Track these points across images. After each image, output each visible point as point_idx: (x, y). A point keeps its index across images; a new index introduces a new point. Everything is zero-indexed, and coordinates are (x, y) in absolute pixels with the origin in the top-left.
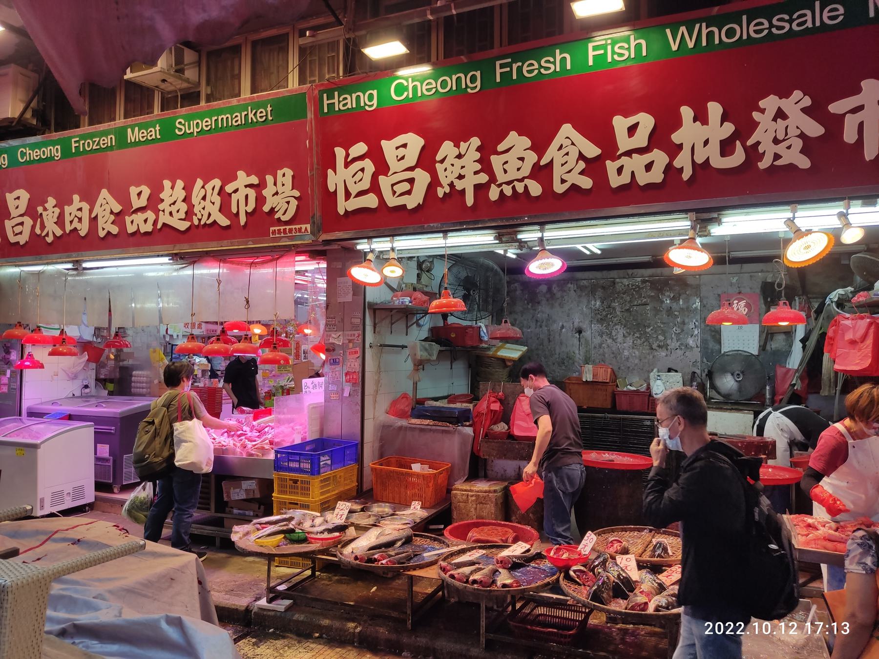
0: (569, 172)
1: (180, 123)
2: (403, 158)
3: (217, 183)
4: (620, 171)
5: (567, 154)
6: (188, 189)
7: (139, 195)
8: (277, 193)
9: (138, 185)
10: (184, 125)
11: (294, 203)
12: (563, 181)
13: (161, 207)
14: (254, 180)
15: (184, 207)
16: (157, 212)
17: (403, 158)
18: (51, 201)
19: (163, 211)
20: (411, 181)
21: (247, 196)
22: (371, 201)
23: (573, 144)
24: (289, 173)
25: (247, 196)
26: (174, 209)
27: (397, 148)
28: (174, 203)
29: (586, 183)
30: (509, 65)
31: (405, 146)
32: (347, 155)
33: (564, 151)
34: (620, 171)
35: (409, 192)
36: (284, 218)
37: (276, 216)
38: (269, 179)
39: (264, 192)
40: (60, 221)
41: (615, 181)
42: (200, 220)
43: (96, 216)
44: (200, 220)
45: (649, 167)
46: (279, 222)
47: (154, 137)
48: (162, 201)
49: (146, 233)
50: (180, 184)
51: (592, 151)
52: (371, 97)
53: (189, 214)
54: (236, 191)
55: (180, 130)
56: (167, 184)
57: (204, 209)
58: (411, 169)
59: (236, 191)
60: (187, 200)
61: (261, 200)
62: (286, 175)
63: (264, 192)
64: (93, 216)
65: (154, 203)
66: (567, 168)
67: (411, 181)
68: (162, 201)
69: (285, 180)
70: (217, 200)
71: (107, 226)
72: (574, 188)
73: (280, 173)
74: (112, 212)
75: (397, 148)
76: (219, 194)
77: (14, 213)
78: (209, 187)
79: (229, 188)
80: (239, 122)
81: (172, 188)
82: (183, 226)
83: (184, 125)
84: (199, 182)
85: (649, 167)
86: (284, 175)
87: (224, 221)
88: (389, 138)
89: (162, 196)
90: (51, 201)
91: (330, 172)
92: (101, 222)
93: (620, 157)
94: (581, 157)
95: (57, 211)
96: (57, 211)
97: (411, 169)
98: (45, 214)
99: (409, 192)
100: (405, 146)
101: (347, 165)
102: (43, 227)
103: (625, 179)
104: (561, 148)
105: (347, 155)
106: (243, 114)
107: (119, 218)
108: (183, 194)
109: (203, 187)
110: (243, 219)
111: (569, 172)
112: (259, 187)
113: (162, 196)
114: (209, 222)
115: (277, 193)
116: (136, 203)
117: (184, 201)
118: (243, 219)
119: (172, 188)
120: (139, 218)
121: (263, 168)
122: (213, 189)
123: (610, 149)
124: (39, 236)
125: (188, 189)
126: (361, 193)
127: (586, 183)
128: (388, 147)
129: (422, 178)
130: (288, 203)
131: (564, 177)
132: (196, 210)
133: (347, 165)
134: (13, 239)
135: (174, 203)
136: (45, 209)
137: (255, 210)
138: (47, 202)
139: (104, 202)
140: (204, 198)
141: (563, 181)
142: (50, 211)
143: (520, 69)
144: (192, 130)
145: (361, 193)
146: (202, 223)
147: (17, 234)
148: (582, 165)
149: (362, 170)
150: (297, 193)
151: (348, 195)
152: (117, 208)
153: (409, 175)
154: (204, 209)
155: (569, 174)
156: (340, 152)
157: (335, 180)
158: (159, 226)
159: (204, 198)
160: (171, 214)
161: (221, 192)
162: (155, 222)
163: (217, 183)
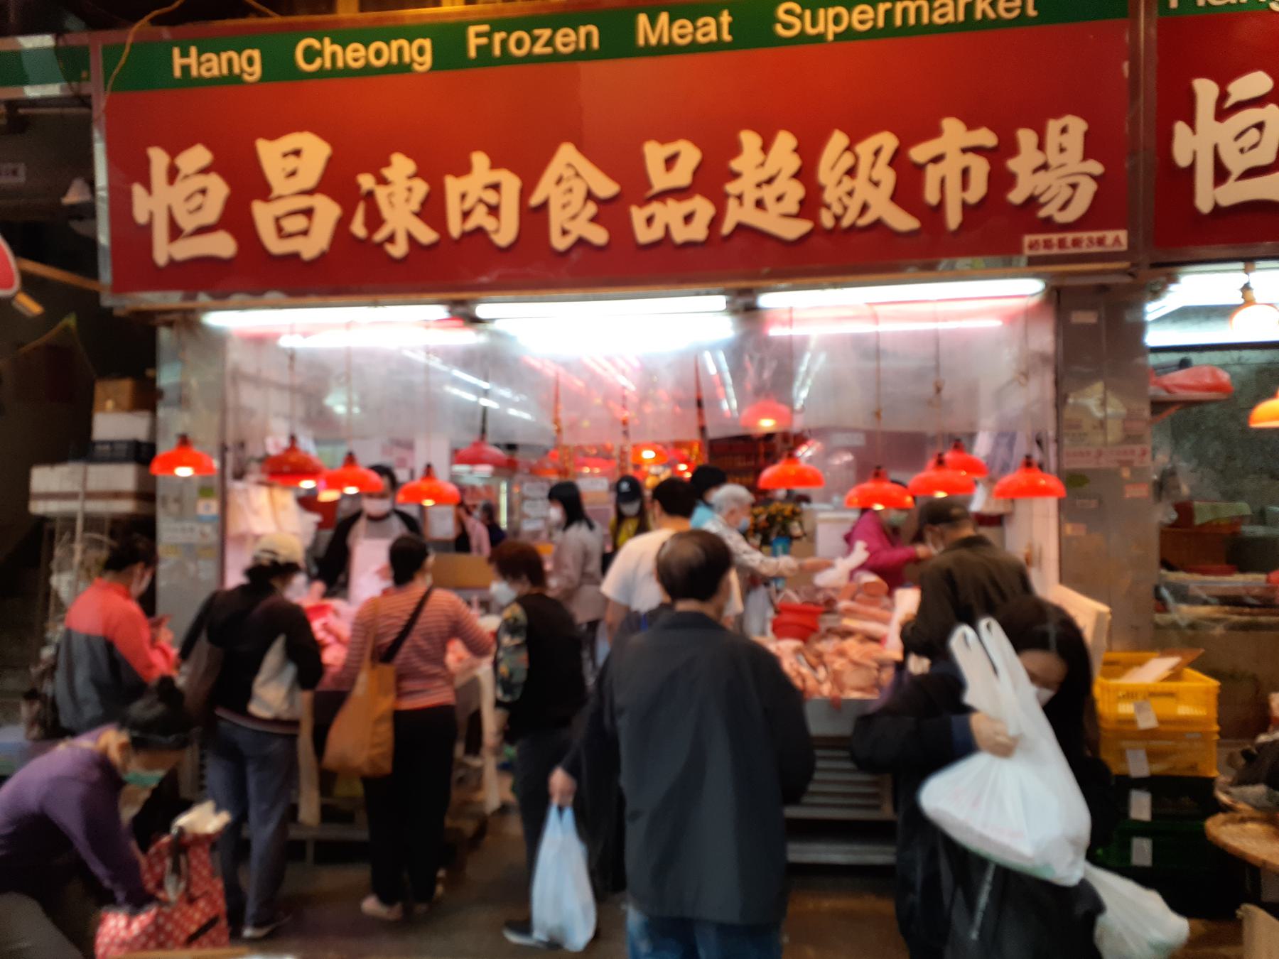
0: (574, 217)
1: (788, 12)
2: (293, 174)
3: (887, 141)
4: (650, 220)
5: (570, 190)
6: (809, 154)
7: (670, 161)
8: (1045, 167)
9: (664, 140)
10: (801, 17)
11: (1088, 189)
12: (565, 232)
13: (732, 188)
14: (986, 137)
15: (796, 191)
16: (720, 200)
17: (293, 174)
18: (401, 166)
19: (740, 197)
20: (308, 213)
21: (965, 172)
22: (223, 245)
23: (577, 175)
24: (1077, 126)
25: (965, 172)
26: (769, 194)
27: (285, 155)
28: (770, 181)
29: (599, 236)
30: (489, 35)
31: (297, 153)
32: (1223, 96)
33: (564, 186)
34: (650, 220)
35: (305, 233)
36: (1062, 218)
37: (1043, 213)
38: (1026, 137)
39: (1013, 164)
40: (432, 210)
41: (645, 235)
42: (838, 218)
43: (544, 206)
44: (838, 218)
45: (688, 218)
46: (1049, 225)
47: (713, 37)
48: (735, 176)
49: (689, 245)
50: (785, 142)
51: (606, 187)
52: (421, 51)
53: (810, 205)
54: (937, 159)
55: (787, 26)
56: (750, 140)
57: (850, 194)
58: (309, 192)
59: (937, 159)
60: (806, 174)
61: (1001, 180)
62: (1069, 132)
63: (1013, 164)
64: (535, 200)
65: (712, 180)
66: (571, 211)
67: (308, 213)
68: (735, 176)
69: (1065, 140)
70: (888, 178)
71: (572, 222)
72: (581, 242)
73: (1053, 126)
74: (590, 196)
75: (285, 155)
76: (891, 163)
77: (279, 184)
78: (865, 148)
79: (919, 153)
80: (950, 18)
81: (766, 148)
82: (794, 229)
83: (801, 17)
84: (838, 140)
85: (688, 218)
86: (1064, 130)
87: (903, 221)
88: (273, 135)
89: (735, 165)
90: (401, 166)
91: (1180, 128)
92: (557, 218)
93: (649, 200)
94: (590, 196)
95: (421, 188)
96: (421, 188)
97: (309, 192)
98: (381, 193)
99: (305, 233)
100: (297, 153)
101: (1222, 113)
102: (375, 219)
103: (655, 233)
104: (559, 181)
105: (1223, 96)
106: (882, 8)
107: (610, 212)
108: (794, 163)
109: (849, 148)
110: (953, 218)
111: (574, 217)
112: (999, 156)
113: (735, 165)
114: (864, 221)
115: (1045, 167)
116: (660, 180)
117: (797, 176)
118: (953, 218)
119: (766, 148)
120: (669, 214)
121: (1008, 113)
122: (877, 153)
123: (635, 188)
124: (366, 243)
125: (809, 154)
126: (202, 230)
127: (599, 236)
128: (270, 153)
129: (327, 211)
130: (1074, 186)
131: (568, 226)
132: (830, 196)
133: (1222, 113)
134: (275, 246)
135: (770, 181)
136: (382, 181)
137: (983, 201)
138: (388, 164)
139: (570, 173)
140: (851, 172)
141: (565, 232)
142: (399, 191)
143: (504, 43)
144: (821, 28)
145: (202, 230)
146: (846, 222)
147: (291, 235)
148: (592, 209)
149: (1260, 126)
150: (1096, 168)
151: (1221, 174)
152: (606, 187)
153: (304, 202)
154: (850, 194)
155: (572, 222)
156: (1206, 90)
157: (1189, 145)
158: (727, 228)
159: (851, 172)
160: (760, 204)
161: (898, 161)
162: (715, 223)
163: (887, 141)
